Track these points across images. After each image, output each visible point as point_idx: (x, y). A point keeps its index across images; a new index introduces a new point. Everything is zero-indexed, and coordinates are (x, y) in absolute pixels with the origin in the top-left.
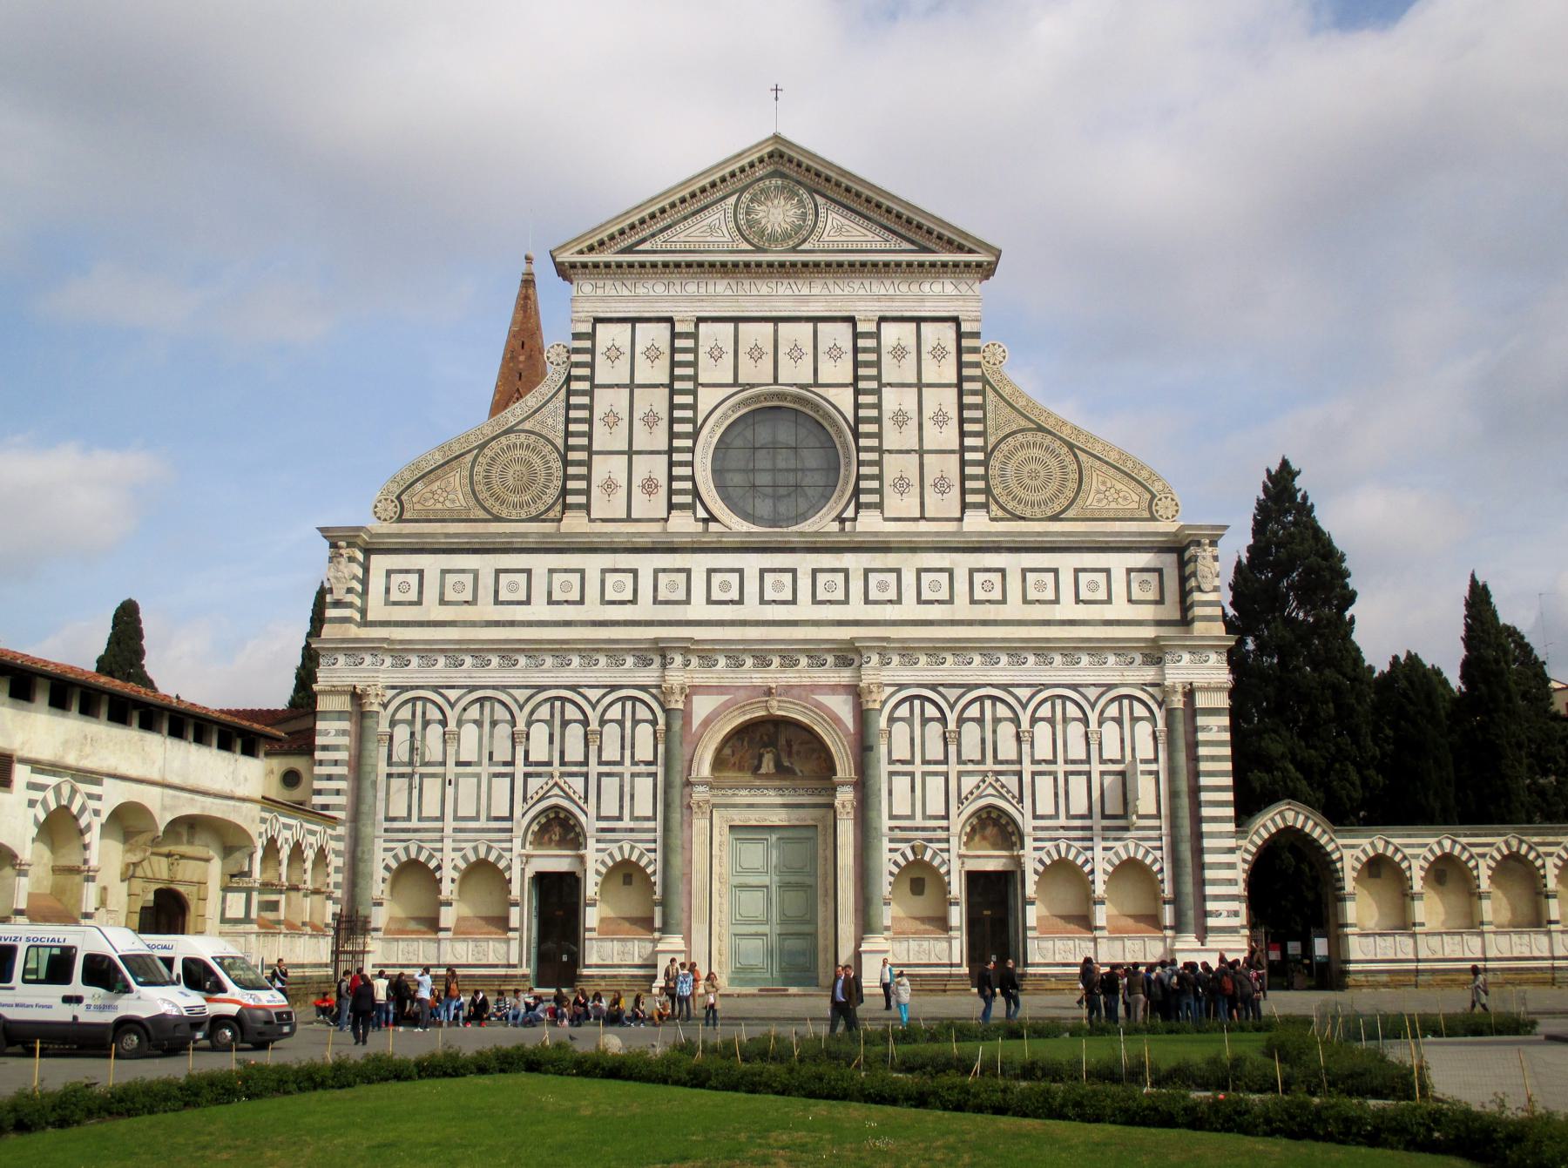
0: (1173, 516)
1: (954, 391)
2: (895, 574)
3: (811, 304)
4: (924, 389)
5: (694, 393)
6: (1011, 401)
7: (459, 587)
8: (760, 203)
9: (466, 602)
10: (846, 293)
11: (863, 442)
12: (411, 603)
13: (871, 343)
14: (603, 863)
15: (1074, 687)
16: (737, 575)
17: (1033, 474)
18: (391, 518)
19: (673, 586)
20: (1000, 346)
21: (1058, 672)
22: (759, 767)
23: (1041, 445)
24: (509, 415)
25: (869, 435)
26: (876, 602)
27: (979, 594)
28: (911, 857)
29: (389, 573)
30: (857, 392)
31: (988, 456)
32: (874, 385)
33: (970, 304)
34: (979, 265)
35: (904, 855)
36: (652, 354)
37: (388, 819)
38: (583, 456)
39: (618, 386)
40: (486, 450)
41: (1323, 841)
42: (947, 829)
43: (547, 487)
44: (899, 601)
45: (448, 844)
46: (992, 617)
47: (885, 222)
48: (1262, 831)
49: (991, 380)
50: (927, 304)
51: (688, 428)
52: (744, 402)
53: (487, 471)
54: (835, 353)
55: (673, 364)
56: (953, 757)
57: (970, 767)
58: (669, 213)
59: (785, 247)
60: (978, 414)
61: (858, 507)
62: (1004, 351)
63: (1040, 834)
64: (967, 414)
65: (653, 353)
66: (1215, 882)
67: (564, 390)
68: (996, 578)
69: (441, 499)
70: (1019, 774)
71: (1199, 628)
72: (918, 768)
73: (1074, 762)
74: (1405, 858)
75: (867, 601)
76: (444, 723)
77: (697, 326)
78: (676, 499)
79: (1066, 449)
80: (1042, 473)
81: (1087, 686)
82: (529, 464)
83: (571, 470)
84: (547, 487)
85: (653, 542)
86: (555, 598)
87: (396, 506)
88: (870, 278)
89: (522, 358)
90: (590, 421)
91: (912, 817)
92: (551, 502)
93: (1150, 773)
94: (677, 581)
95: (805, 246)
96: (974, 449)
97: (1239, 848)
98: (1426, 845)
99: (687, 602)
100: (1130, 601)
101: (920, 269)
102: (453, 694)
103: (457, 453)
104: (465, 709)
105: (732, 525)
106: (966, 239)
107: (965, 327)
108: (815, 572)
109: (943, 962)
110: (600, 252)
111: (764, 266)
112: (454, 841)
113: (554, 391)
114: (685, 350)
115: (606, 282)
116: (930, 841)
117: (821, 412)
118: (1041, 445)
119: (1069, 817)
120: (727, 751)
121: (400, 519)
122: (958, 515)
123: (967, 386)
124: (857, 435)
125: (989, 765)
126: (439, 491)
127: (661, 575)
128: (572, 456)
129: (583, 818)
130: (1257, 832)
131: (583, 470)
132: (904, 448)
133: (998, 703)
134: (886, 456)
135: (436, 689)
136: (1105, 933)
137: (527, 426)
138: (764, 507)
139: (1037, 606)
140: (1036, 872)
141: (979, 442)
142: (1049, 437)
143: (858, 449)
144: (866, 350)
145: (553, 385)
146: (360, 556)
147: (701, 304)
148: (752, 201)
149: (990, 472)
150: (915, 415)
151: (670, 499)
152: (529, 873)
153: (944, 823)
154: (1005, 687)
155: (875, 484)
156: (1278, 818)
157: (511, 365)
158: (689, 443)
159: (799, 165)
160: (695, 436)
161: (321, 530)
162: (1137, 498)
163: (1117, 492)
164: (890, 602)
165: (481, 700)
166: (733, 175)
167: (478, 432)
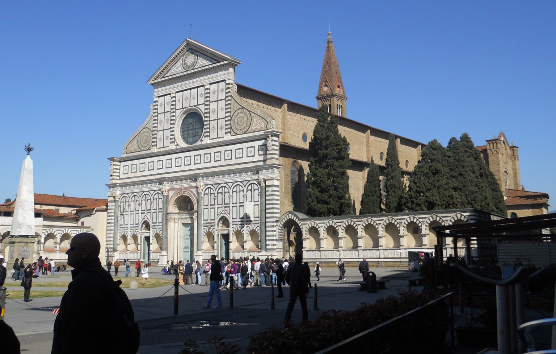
5: (175, 112)
8: (187, 58)
11: (206, 119)
14: (153, 234)
15: (241, 182)
21: (238, 178)
22: (187, 208)
28: (208, 231)
35: (206, 230)
37: (120, 225)
38: (156, 132)
41: (298, 223)
42: (214, 223)
45: (129, 230)
46: (229, 164)
48: (283, 220)
51: (174, 122)
53: (140, 139)
56: (216, 203)
57: (220, 206)
59: (192, 68)
61: (206, 136)
63: (234, 223)
66: (269, 236)
70: (229, 207)
71: (268, 162)
72: (209, 207)
73: (241, 203)
74: (319, 227)
76: (128, 202)
81: (244, 181)
82: (147, 136)
83: (154, 136)
90: (157, 123)
91: (207, 220)
93: (258, 205)
97: (277, 225)
98: (324, 223)
100: (259, 155)
102: (129, 195)
104: (132, 198)
109: (357, 257)
112: (130, 230)
116: (211, 226)
119: (239, 218)
120: (182, 204)
121: (127, 153)
123: (227, 99)
125: (223, 205)
128: (154, 133)
129: (150, 223)
130: (282, 220)
133: (226, 188)
134: (211, 122)
135: (127, 194)
136: (246, 250)
137: (146, 127)
138: (190, 140)
140: (233, 234)
141: (229, 114)
146: (118, 163)
148: (185, 58)
152: (143, 237)
153: (213, 221)
154: (226, 183)
155: (208, 130)
156: (287, 216)
162: (264, 124)
165: (134, 196)
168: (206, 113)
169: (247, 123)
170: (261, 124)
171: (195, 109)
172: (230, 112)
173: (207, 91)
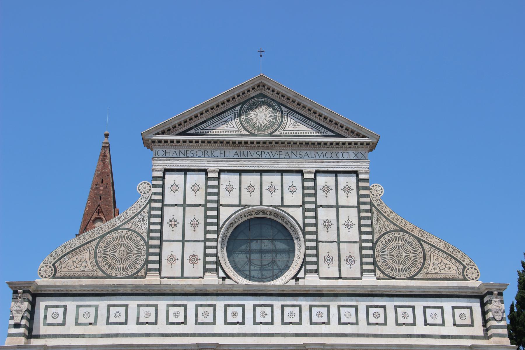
0: (476, 278)
1: (356, 210)
2: (326, 308)
3: (279, 163)
4: (340, 209)
5: (218, 209)
6: (386, 215)
7: (87, 315)
9: (91, 324)
10: (298, 158)
11: (308, 237)
12: (59, 324)
13: (311, 184)
16: (241, 308)
17: (399, 255)
18: (49, 276)
19: (206, 314)
20: (379, 186)
23: (403, 239)
24: (117, 220)
25: (310, 233)
26: (316, 324)
27: (372, 320)
29: (46, 307)
30: (305, 210)
31: (375, 244)
32: (313, 206)
33: (364, 164)
34: (368, 144)
36: (196, 188)
38: (157, 242)
39: (176, 205)
40: (104, 239)
43: (138, 260)
44: (329, 323)
47: (318, 121)
49: (375, 204)
50: (341, 164)
51: (215, 228)
52: (245, 214)
54: (292, 189)
55: (207, 194)
58: (205, 114)
59: (266, 133)
60: (369, 222)
61: (306, 271)
62: (382, 189)
64: (363, 222)
65: (196, 188)
67: (148, 207)
68: (381, 311)
69: (78, 266)
75: (311, 323)
77: (219, 175)
78: (208, 266)
79: (416, 241)
80: (404, 254)
82: (128, 247)
83: (151, 250)
84: (138, 260)
85: (195, 290)
86: (141, 321)
87: (52, 270)
88: (311, 150)
89: (102, 188)
90: (161, 224)
92: (140, 267)
94: (209, 312)
95: (276, 133)
96: (367, 241)
99: (214, 323)
100: (455, 325)
101: (337, 146)
103: (88, 240)
105: (238, 281)
106: (361, 130)
107: (361, 176)
108: (283, 306)
110: (168, 134)
111: (255, 143)
113: (142, 208)
114: (213, 187)
115: (171, 150)
117: (285, 220)
118: (403, 239)
121: (54, 277)
122: (359, 276)
123: (362, 207)
124: (304, 233)
126: (77, 261)
127: (199, 308)
128: (152, 242)
131: (157, 250)
132: (330, 240)
134: (320, 244)
137: (127, 226)
139: (404, 326)
141: (369, 237)
142: (407, 234)
143: (306, 241)
144: (308, 188)
145: (142, 204)
146: (30, 298)
147: (222, 163)
149: (376, 253)
150: (335, 222)
151: (204, 267)
155: (314, 259)
157: (96, 191)
158: (215, 236)
159: (273, 91)
160: (217, 232)
161: (9, 283)
162: (455, 268)
163: (445, 264)
164: (324, 323)
166: (239, 96)
167: (100, 229)
168: (305, 225)
169: (415, 261)
170: (450, 268)
171: (273, 213)
172: (371, 233)
173: (306, 184)
